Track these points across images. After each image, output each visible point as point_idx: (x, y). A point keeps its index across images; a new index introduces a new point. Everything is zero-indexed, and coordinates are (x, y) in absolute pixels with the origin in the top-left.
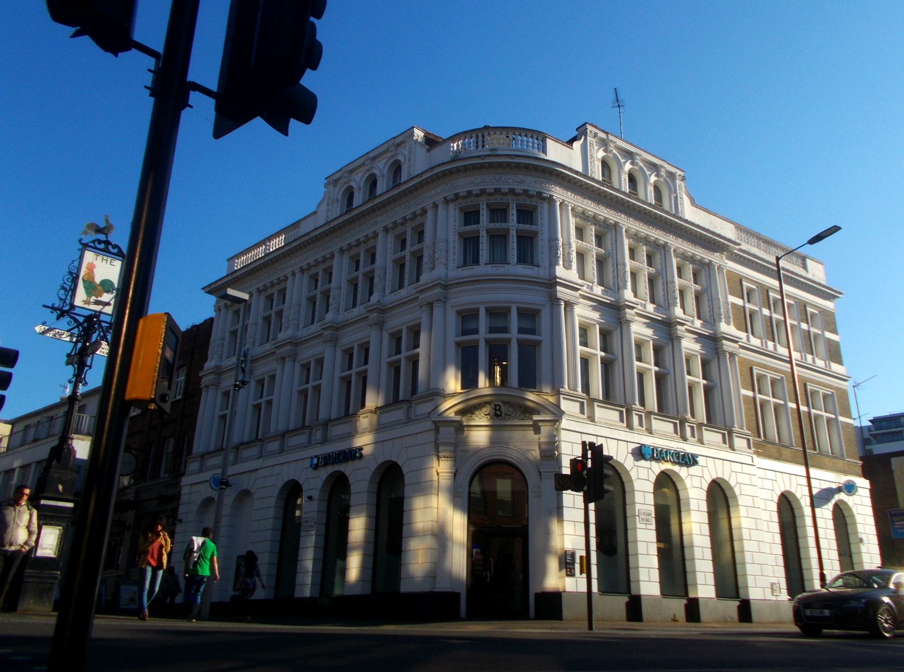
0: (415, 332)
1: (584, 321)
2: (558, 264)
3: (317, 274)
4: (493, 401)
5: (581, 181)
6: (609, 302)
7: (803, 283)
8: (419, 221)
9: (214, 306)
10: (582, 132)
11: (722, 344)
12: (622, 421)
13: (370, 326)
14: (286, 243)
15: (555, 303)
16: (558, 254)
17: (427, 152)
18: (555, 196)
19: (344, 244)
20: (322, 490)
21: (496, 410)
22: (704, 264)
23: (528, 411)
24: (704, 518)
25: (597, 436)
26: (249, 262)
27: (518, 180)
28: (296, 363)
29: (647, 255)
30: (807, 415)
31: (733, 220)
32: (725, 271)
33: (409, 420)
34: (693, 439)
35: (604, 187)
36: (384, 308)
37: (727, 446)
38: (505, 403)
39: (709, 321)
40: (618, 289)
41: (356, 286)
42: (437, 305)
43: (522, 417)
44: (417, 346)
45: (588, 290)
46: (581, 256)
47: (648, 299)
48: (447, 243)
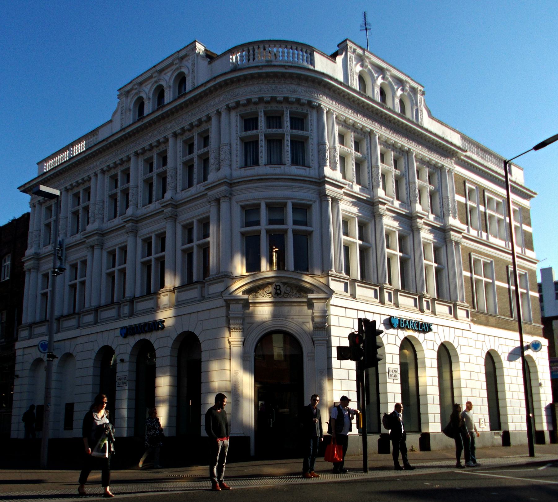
0: (205, 224)
2: (325, 165)
3: (116, 175)
4: (274, 283)
5: (344, 91)
6: (365, 198)
8: (204, 127)
10: (342, 48)
13: (166, 219)
14: (87, 148)
15: (324, 199)
16: (325, 156)
18: (323, 105)
19: (139, 148)
21: (276, 289)
22: (437, 168)
23: (303, 290)
24: (435, 372)
26: (56, 165)
27: (291, 90)
31: (460, 131)
35: (363, 97)
38: (284, 284)
40: (372, 188)
41: (151, 185)
42: (223, 200)
43: (298, 295)
44: (207, 235)
48: (230, 147)
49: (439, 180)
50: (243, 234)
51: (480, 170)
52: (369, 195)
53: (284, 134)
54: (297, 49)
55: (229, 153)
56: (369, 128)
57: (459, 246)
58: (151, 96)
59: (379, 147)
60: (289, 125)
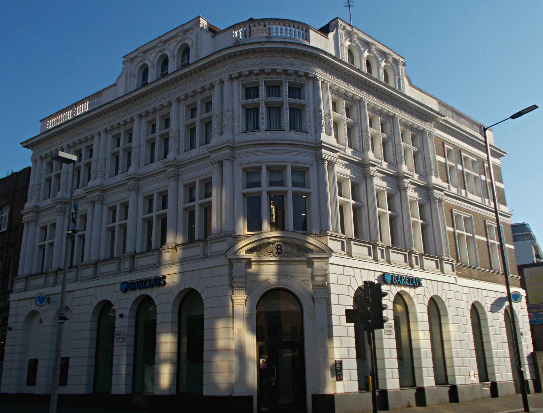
0: (207, 184)
2: (322, 131)
5: (337, 64)
6: (357, 161)
8: (207, 94)
9: (31, 158)
11: (434, 193)
12: (370, 255)
13: (168, 178)
14: (91, 109)
16: (321, 123)
17: (212, 38)
18: (319, 76)
19: (143, 111)
20: (131, 309)
21: (277, 249)
22: (419, 131)
23: (303, 249)
25: (354, 267)
27: (290, 63)
28: (104, 205)
29: (381, 124)
33: (205, 256)
34: (417, 266)
35: (353, 70)
36: (180, 164)
37: (440, 270)
39: (423, 175)
50: (244, 195)
53: (284, 102)
54: (294, 27)
55: (231, 119)
58: (155, 64)
59: (367, 113)
60: (287, 94)
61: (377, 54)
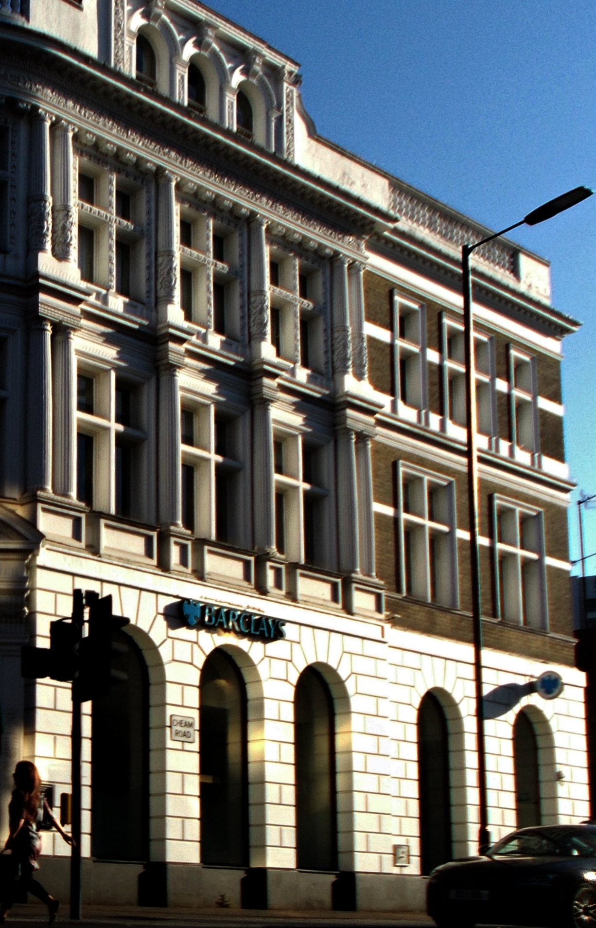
1: (86, 364)
2: (42, 249)
6: (136, 327)
7: (508, 301)
16: (43, 228)
30: (487, 554)
32: (362, 273)
34: (277, 591)
45: (99, 303)
46: (88, 234)
47: (212, 324)
49: (325, 288)
51: (433, 263)
52: (147, 319)
56: (155, 164)
57: (366, 445)
61: (221, 50)
